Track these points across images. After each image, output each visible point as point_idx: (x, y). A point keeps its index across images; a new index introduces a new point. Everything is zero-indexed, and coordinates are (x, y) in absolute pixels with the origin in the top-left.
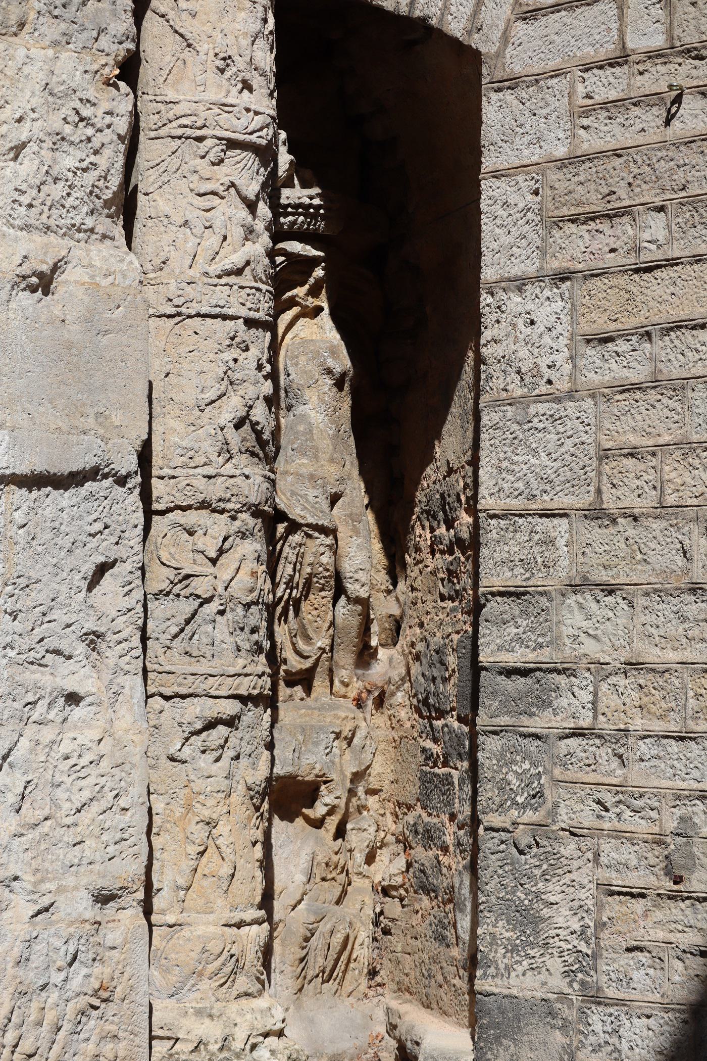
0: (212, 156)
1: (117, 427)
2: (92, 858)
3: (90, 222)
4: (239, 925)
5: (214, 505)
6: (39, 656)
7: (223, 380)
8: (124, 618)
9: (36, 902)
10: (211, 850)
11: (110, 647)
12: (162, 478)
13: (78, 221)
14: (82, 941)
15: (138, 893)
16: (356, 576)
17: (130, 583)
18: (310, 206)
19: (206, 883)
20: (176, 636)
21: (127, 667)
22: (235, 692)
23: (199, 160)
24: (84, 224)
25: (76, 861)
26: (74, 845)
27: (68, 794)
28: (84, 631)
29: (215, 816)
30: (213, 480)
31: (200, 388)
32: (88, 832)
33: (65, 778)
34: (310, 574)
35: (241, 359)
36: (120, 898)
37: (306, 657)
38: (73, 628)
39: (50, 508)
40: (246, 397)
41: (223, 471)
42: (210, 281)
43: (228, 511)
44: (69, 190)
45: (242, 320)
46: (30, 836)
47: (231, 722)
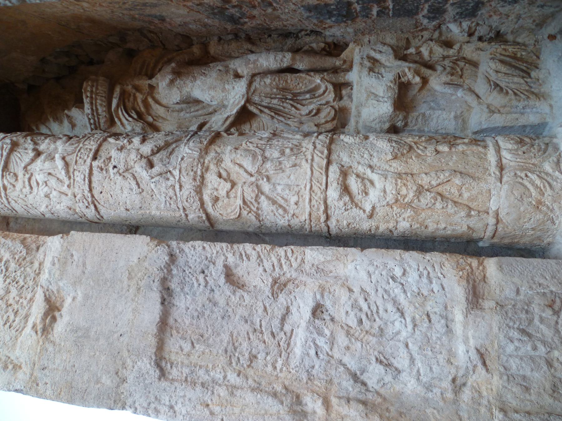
0: (12, 181)
1: (139, 262)
2: (441, 307)
3: (36, 265)
4: (501, 168)
5: (198, 183)
6: (284, 337)
7: (124, 176)
8: (265, 261)
9: (475, 366)
10: (440, 189)
11: (284, 274)
12: (186, 215)
13: (32, 275)
14: (511, 324)
15: (473, 265)
16: (279, 61)
17: (241, 254)
18: (91, 97)
19: (466, 195)
20: (285, 210)
21: (299, 260)
22: (324, 169)
23: (17, 188)
24: (35, 271)
25: (443, 321)
26: (430, 321)
27: (389, 323)
28: (270, 296)
29: (415, 188)
30: (183, 184)
31: (130, 191)
32: (421, 309)
33: (376, 326)
34: (277, 89)
35: (114, 164)
36: (475, 281)
37: (327, 89)
38: (267, 305)
39: (184, 318)
40: (135, 159)
41: (177, 178)
42: (72, 184)
43: (202, 173)
44: (15, 283)
45: (93, 163)
46: (420, 365)
47: (344, 174)
